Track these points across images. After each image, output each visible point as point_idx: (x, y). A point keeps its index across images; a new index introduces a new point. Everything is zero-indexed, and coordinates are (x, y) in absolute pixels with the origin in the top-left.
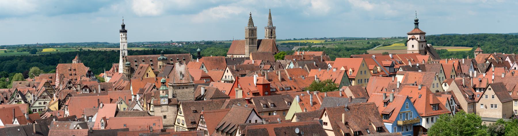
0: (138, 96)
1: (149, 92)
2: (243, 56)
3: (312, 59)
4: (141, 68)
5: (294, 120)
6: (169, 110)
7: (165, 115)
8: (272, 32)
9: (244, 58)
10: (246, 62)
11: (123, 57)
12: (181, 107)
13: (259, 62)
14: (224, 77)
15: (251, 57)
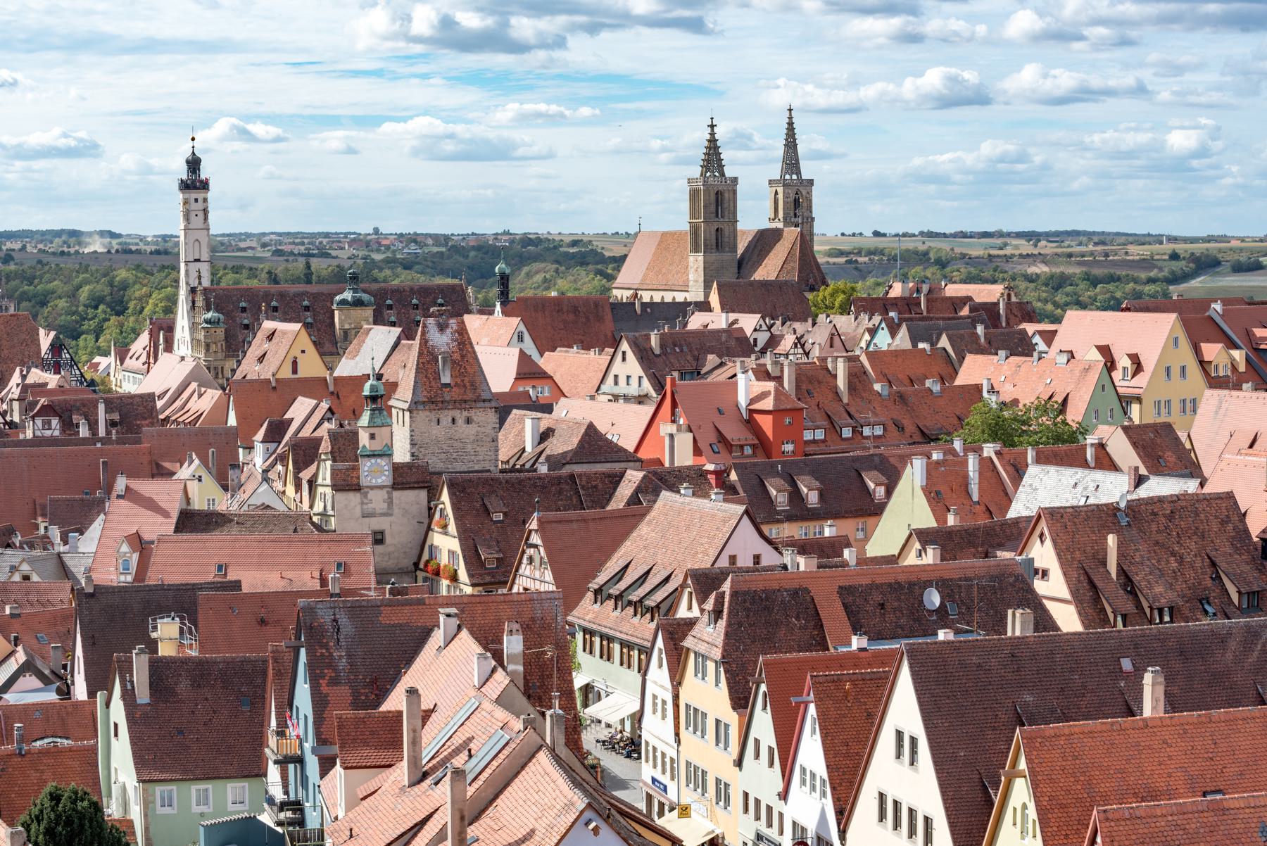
0: (259, 448)
1: (306, 433)
2: (680, 297)
3: (965, 311)
4: (271, 337)
5: (911, 559)
6: (396, 511)
7: (377, 528)
8: (797, 203)
9: (686, 304)
10: (696, 321)
11: (193, 291)
12: (445, 496)
13: (748, 322)
14: (610, 379)
15: (714, 299)
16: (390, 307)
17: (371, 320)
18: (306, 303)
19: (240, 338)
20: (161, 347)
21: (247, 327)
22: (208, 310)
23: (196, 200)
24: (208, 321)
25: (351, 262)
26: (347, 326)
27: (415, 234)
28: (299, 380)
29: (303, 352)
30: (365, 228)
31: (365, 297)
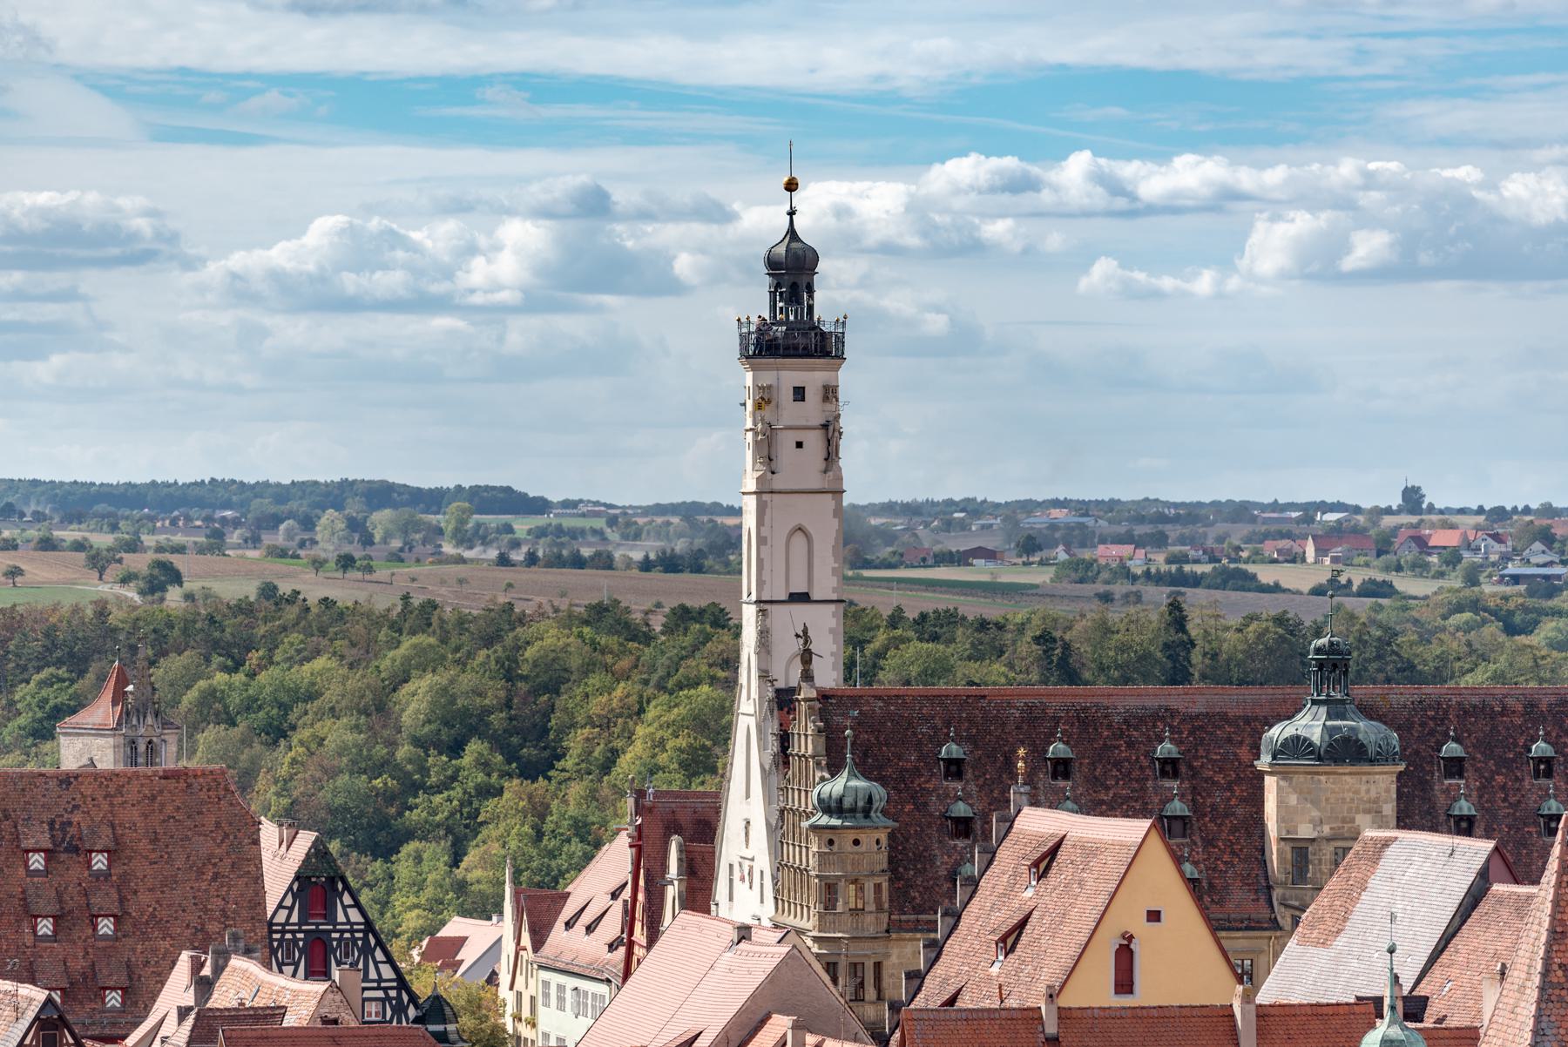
4: (1045, 861)
11: (783, 701)
16: (1455, 767)
17: (1389, 809)
18: (1166, 749)
19: (942, 864)
20: (671, 892)
21: (963, 827)
22: (834, 769)
23: (799, 393)
24: (832, 807)
25: (1325, 603)
26: (1305, 831)
27: (1548, 510)
28: (1139, 1013)
29: (1154, 916)
30: (1373, 489)
31: (1367, 730)
